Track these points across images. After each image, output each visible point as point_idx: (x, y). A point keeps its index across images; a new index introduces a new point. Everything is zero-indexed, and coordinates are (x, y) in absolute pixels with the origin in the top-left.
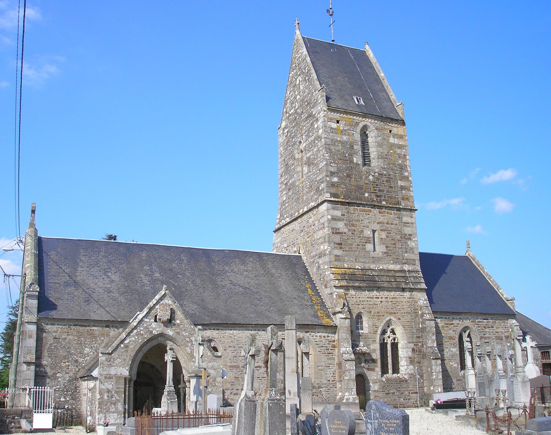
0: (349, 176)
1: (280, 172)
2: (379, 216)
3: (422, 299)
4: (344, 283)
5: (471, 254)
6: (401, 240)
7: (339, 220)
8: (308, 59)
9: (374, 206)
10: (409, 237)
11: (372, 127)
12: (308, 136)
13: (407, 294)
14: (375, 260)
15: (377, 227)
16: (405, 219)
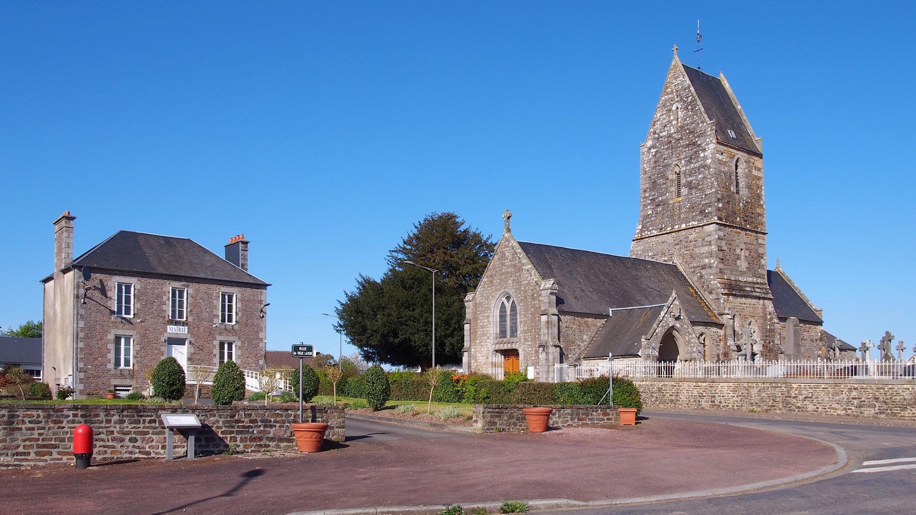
0: (728, 202)
1: (643, 187)
2: (745, 237)
3: (770, 307)
4: (726, 291)
5: (781, 270)
6: (756, 257)
7: (722, 239)
8: (692, 89)
9: (743, 229)
10: (761, 256)
11: (742, 160)
12: (689, 162)
13: (761, 302)
14: (742, 273)
15: (743, 246)
16: (760, 241)
